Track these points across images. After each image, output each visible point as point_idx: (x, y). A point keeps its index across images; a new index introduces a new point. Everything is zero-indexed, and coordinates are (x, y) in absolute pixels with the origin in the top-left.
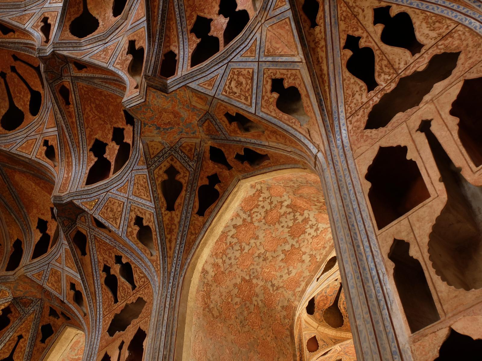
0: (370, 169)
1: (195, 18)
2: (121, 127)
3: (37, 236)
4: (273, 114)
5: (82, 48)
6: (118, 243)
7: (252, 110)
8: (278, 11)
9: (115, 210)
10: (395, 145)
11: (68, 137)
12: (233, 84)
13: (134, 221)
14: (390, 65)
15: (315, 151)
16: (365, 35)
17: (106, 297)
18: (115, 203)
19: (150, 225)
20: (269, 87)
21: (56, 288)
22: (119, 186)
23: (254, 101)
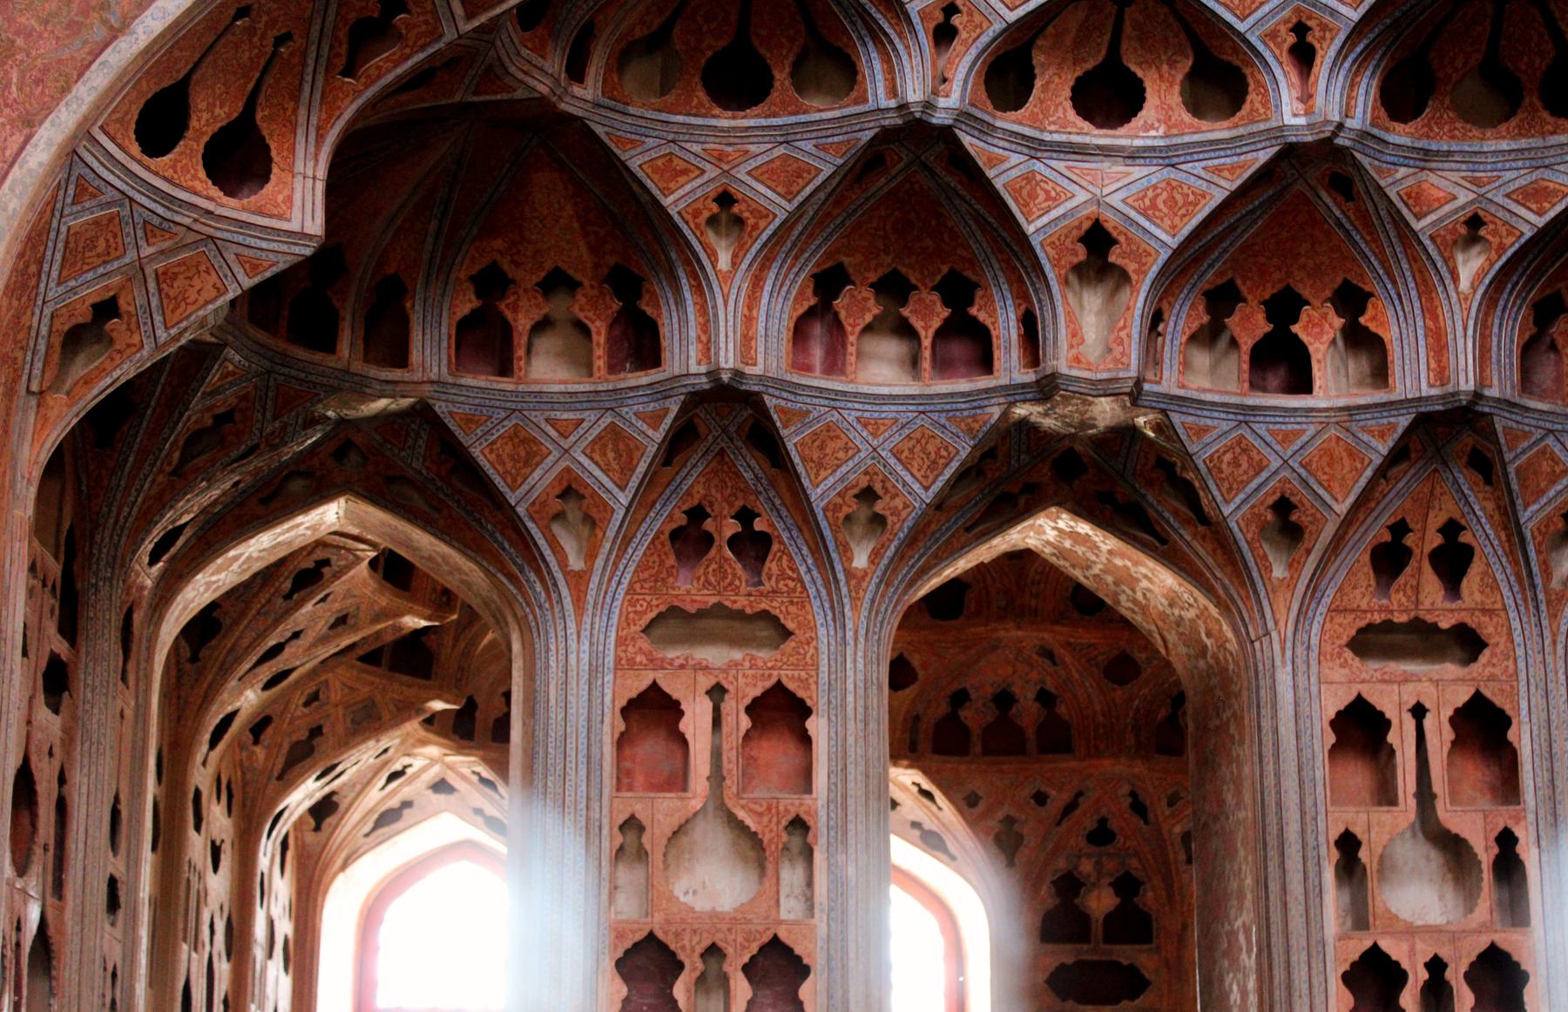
0: (1339, 713)
1: (1225, 279)
2: (913, 281)
3: (467, 304)
4: (1249, 536)
5: (990, 140)
6: (772, 493)
7: (1226, 511)
8: (1365, 437)
9: (828, 451)
10: (1378, 708)
11: (796, 232)
12: (1228, 457)
13: (856, 491)
14: (1417, 589)
15: (1270, 624)
16: (1420, 534)
17: (655, 557)
18: (838, 437)
19: (890, 520)
20: (1271, 500)
21: (507, 472)
22: (867, 415)
23: (1238, 500)
